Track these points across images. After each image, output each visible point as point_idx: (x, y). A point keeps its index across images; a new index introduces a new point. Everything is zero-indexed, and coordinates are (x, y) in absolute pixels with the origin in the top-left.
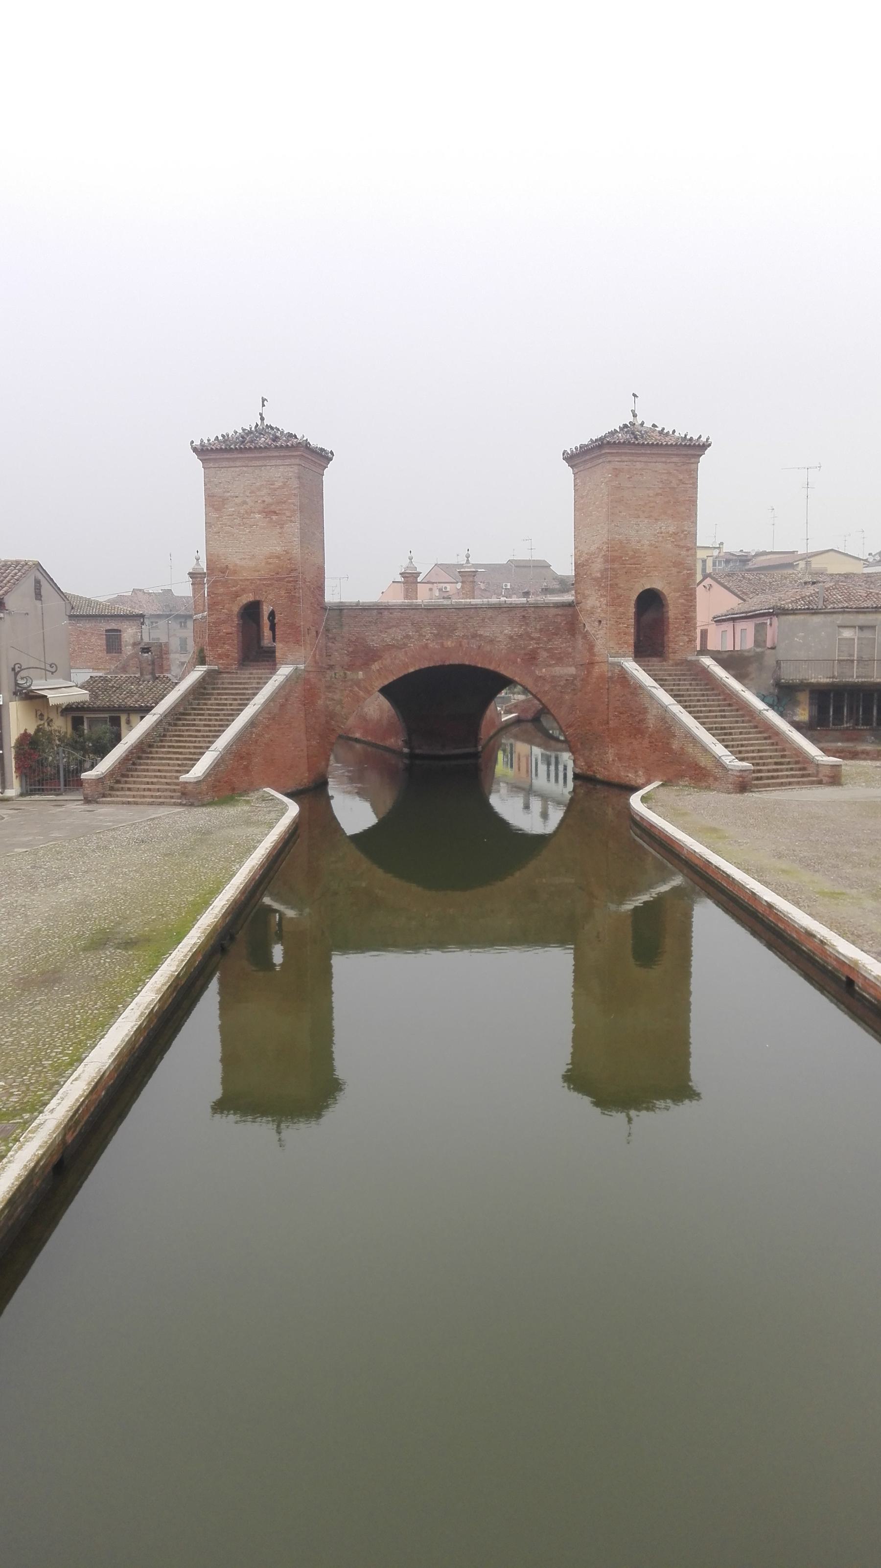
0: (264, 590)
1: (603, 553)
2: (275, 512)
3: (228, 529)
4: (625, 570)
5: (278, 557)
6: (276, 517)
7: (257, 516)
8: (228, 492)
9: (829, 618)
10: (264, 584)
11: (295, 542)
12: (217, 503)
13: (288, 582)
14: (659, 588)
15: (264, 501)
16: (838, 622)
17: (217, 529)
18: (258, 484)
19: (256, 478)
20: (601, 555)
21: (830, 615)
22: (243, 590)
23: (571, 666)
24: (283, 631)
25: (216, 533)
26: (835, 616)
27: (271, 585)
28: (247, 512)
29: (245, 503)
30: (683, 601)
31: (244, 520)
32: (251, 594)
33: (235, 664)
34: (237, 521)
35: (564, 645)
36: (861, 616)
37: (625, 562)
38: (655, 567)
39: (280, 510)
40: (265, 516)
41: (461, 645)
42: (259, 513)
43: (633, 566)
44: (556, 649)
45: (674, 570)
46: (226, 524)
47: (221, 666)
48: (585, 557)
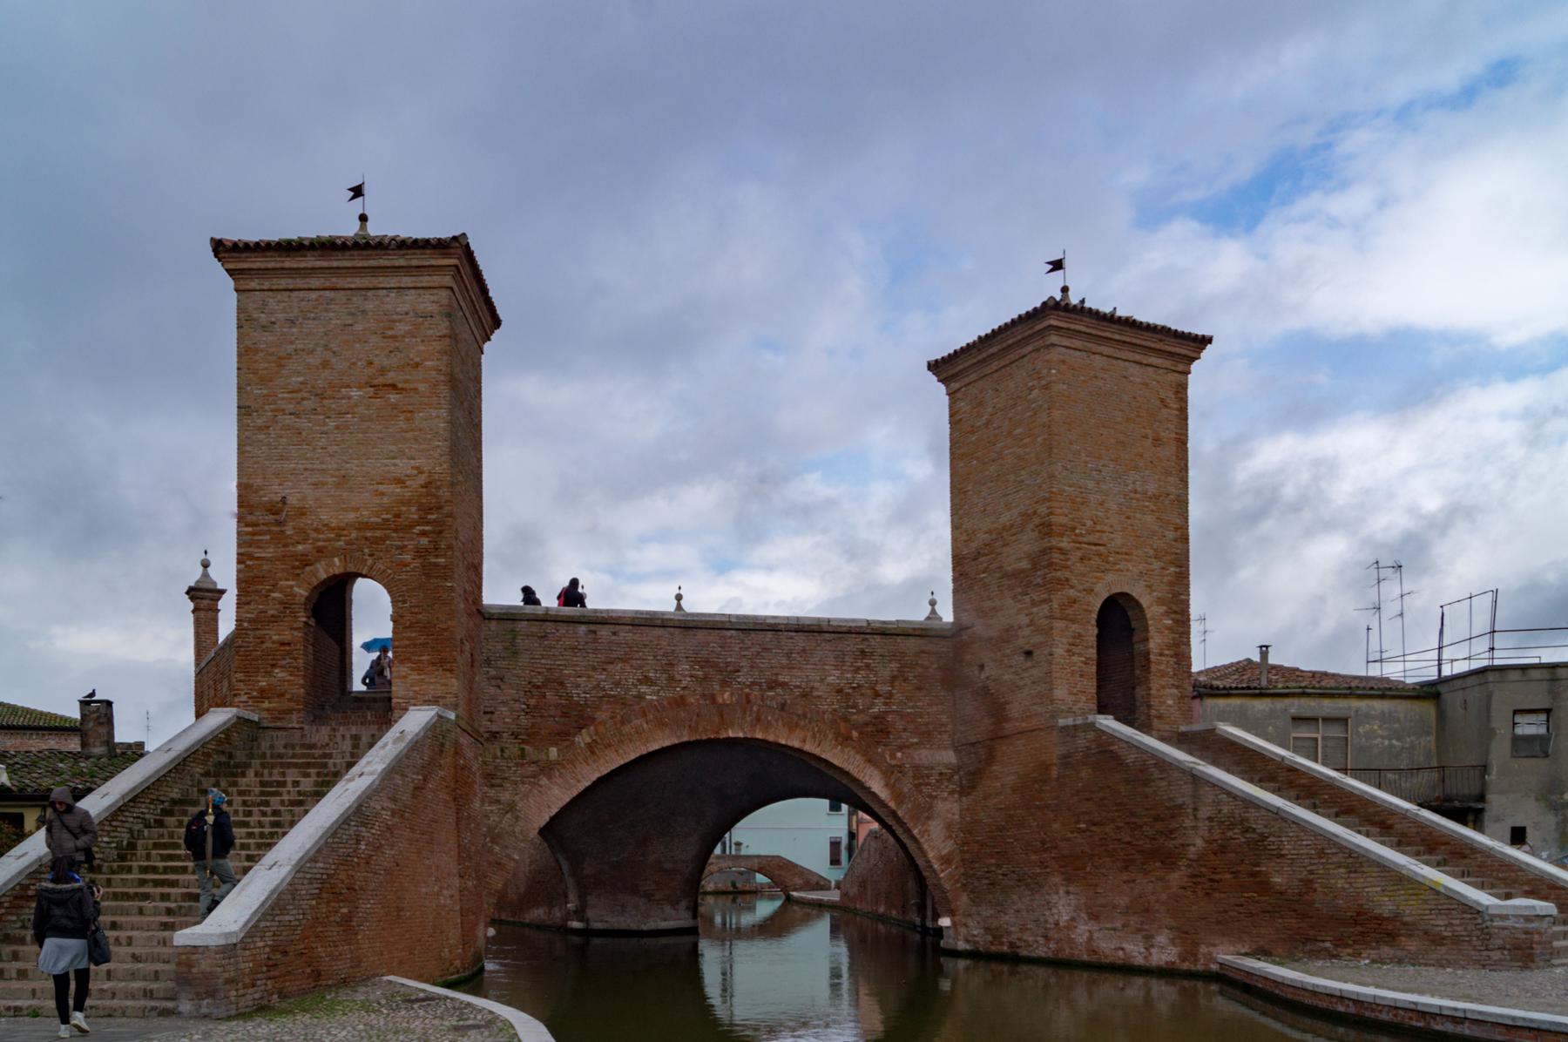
0: (366, 551)
1: (1037, 521)
2: (394, 386)
3: (289, 420)
4: (1079, 554)
5: (399, 481)
6: (398, 396)
7: (355, 393)
8: (292, 343)
9: (1280, 704)
10: (366, 538)
11: (439, 451)
12: (266, 365)
13: (423, 534)
14: (1134, 595)
15: (371, 363)
16: (1293, 711)
17: (264, 418)
20: (1031, 526)
21: (1280, 699)
25: (260, 428)
26: (1287, 701)
27: (383, 539)
29: (325, 364)
30: (1170, 622)
33: (299, 711)
34: (308, 404)
36: (1326, 702)
37: (1080, 539)
38: (1126, 554)
39: (406, 381)
40: (371, 394)
41: (749, 701)
42: (360, 387)
43: (1093, 548)
45: (1157, 565)
46: (283, 410)
47: (265, 715)
48: (982, 537)
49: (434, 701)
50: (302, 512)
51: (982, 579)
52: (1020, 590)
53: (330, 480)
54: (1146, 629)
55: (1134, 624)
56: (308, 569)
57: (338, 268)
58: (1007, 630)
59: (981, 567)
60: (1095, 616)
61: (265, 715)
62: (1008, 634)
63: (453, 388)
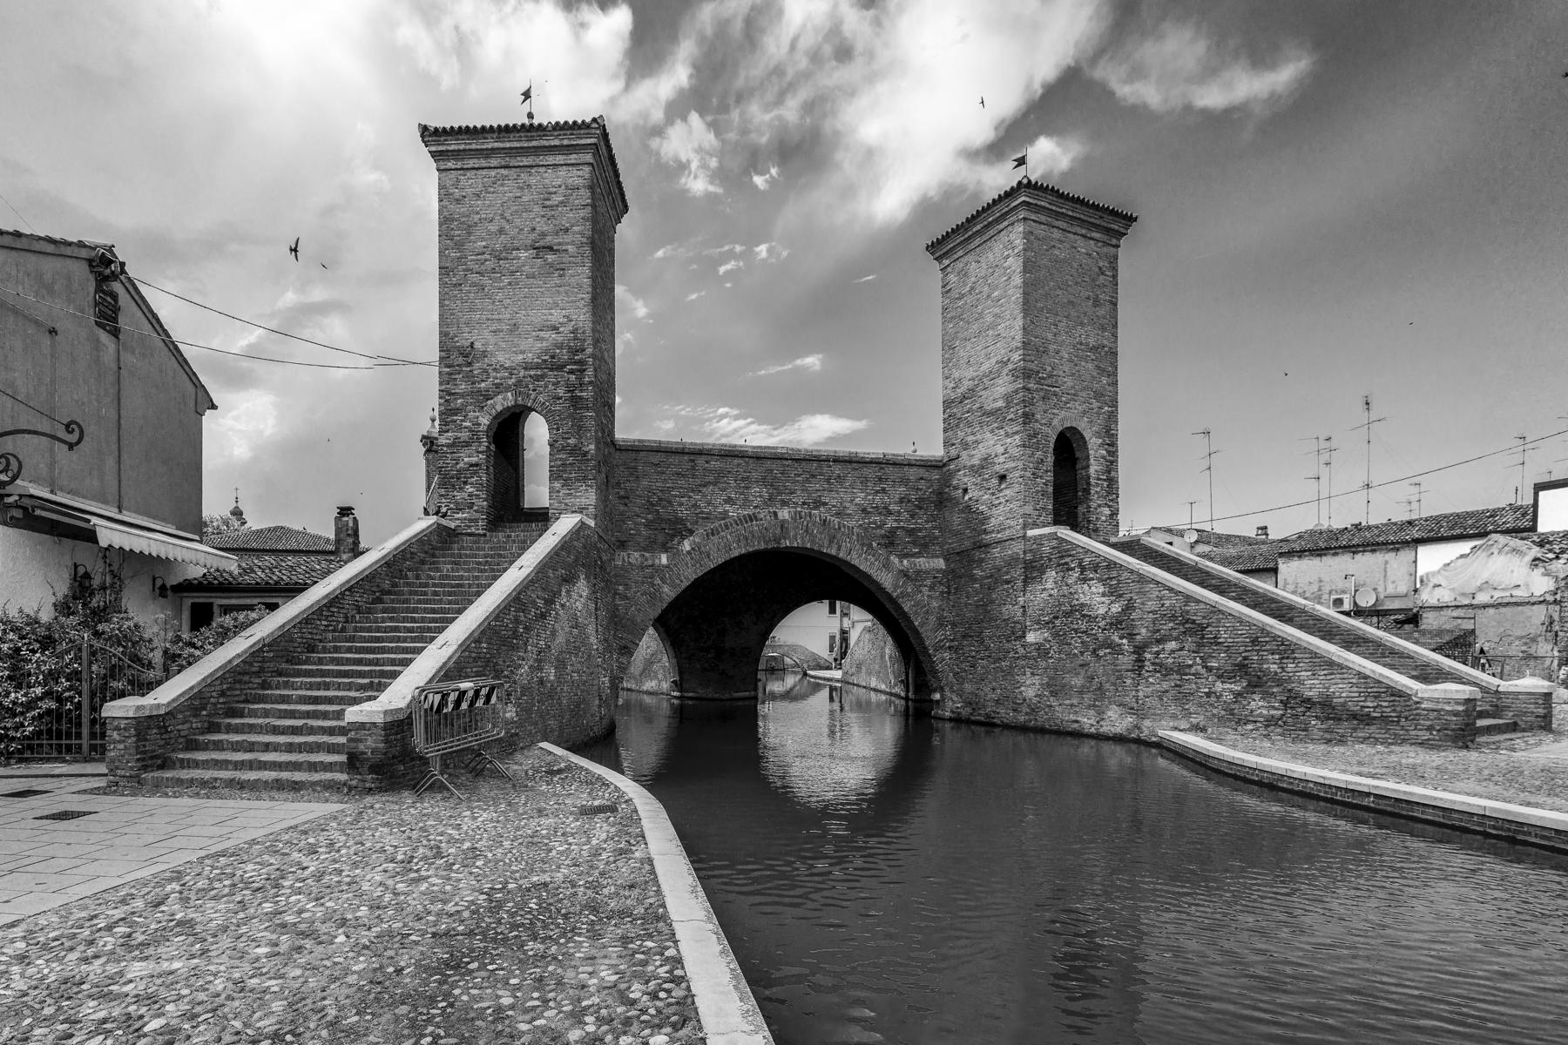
7: (523, 254)
18: (525, 199)
19: (522, 188)
22: (497, 386)
23: (938, 557)
24: (561, 459)
28: (506, 249)
29: (501, 231)
31: (501, 262)
32: (509, 394)
35: (930, 525)
42: (526, 250)
44: (920, 530)
48: (967, 384)
49: (581, 510)
50: (484, 354)
51: (966, 418)
52: (996, 425)
53: (505, 327)
54: (1088, 458)
55: (1078, 454)
56: (489, 402)
57: (510, 148)
58: (986, 459)
59: (966, 409)
60: (1052, 445)
61: (458, 522)
62: (987, 461)
63: (593, 249)
